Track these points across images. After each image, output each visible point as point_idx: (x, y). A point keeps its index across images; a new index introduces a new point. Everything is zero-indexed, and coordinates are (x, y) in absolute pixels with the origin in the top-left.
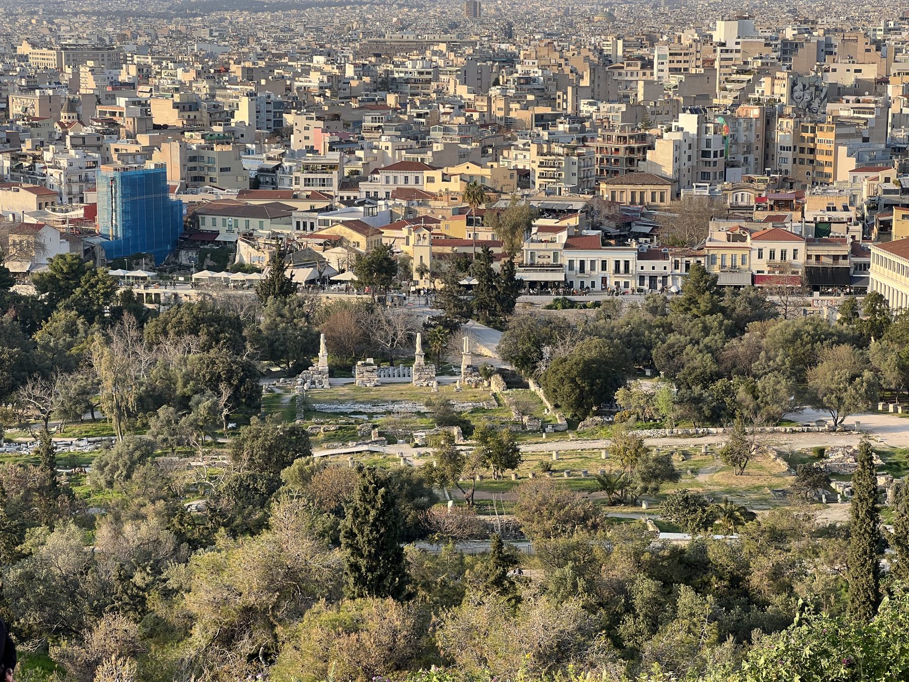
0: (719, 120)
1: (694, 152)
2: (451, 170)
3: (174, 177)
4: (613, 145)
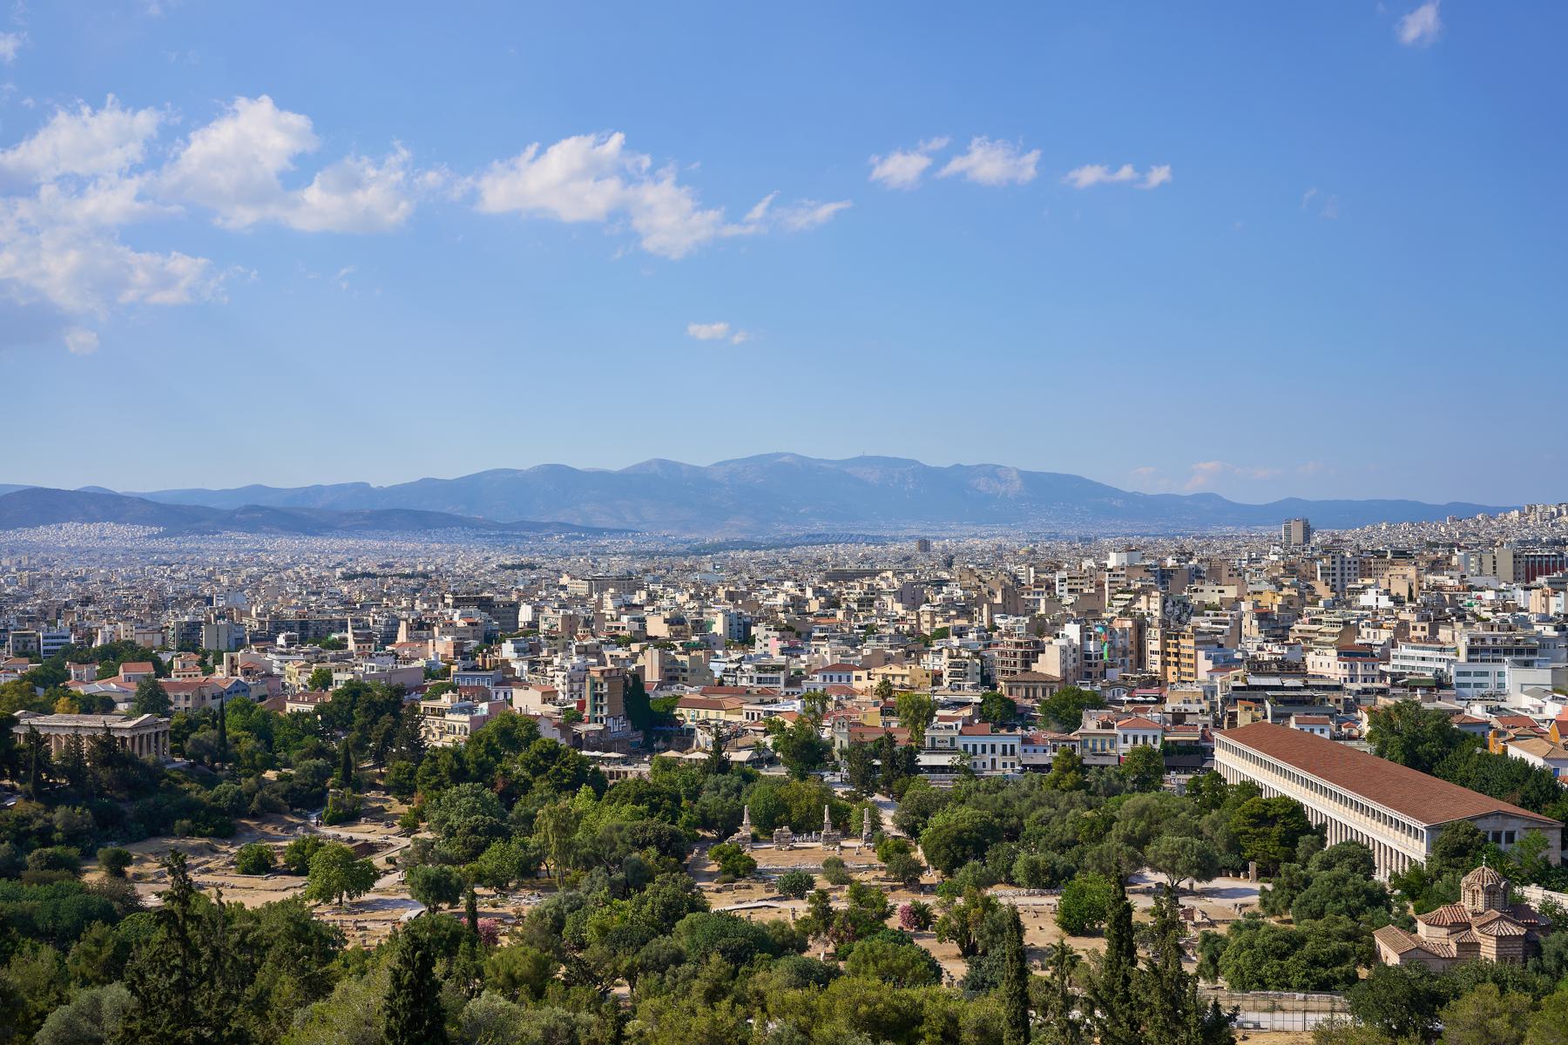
0: (1098, 630)
1: (1078, 655)
2: (878, 671)
3: (652, 675)
4: (1011, 649)
